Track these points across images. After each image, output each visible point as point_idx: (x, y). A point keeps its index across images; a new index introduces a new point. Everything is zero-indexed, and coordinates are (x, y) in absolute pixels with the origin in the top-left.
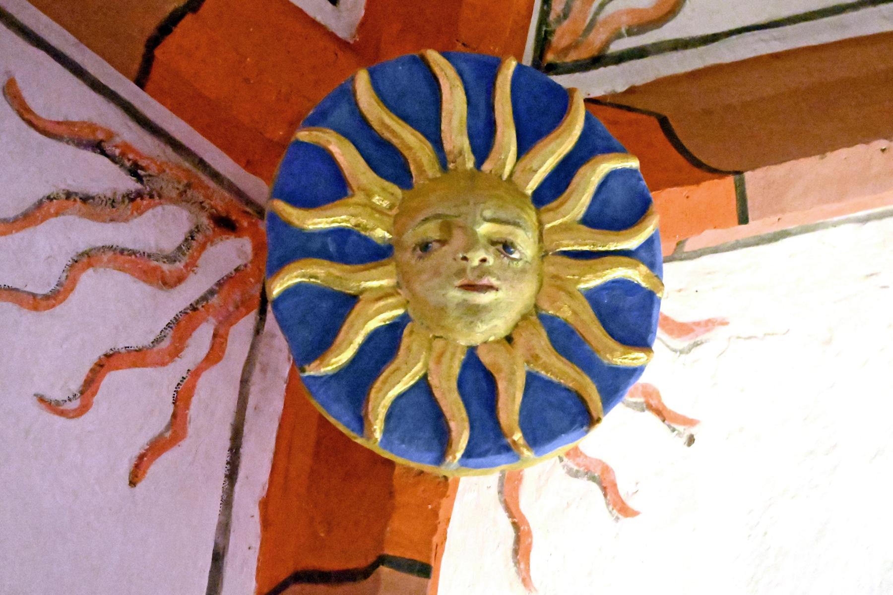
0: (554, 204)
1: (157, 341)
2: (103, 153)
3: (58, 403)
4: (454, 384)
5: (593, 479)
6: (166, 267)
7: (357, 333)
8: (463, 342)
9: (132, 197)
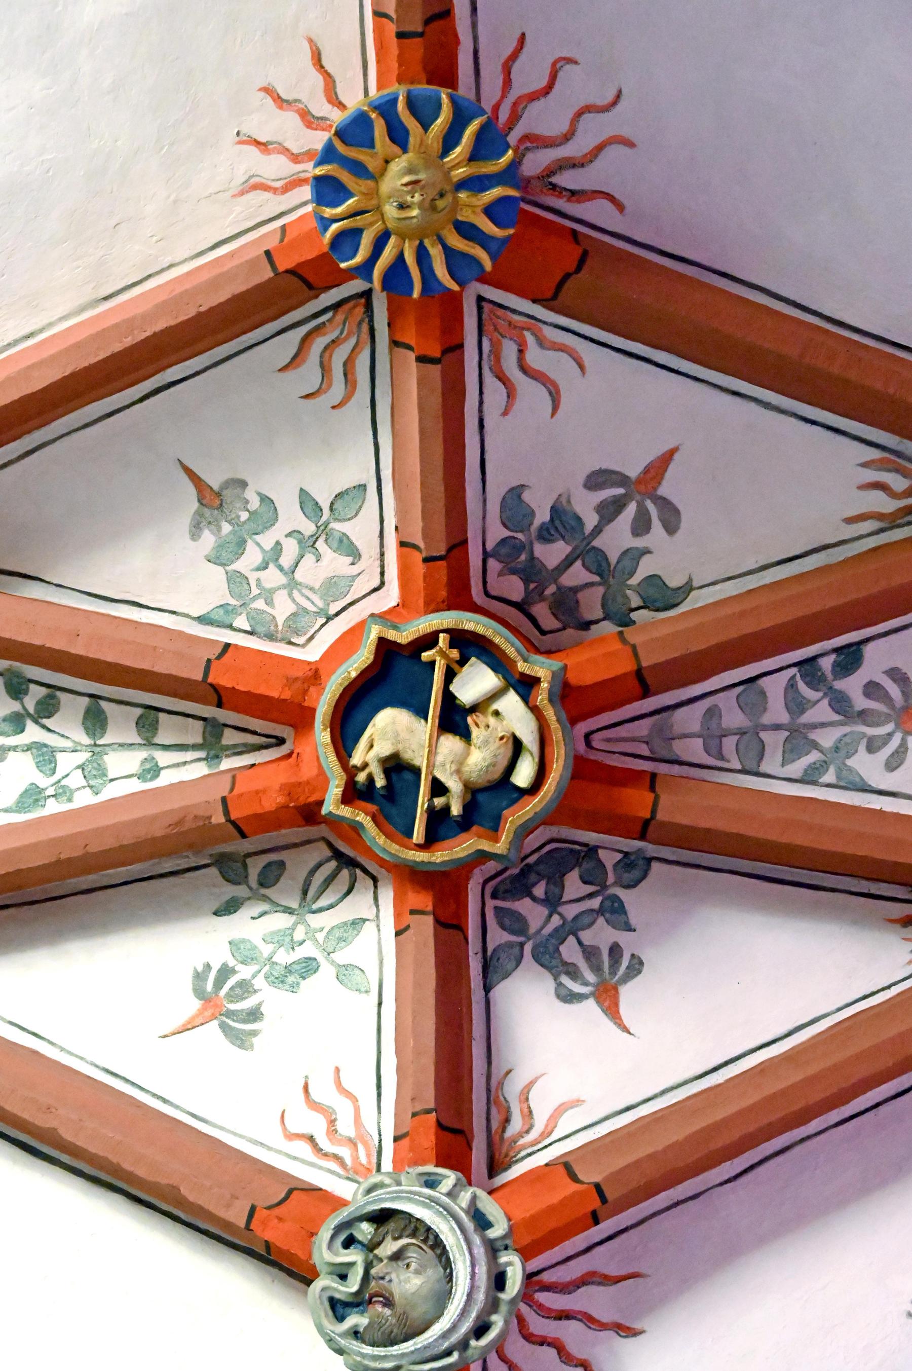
0: (379, 234)
1: (526, 107)
2: (570, 191)
3: (568, 63)
4: (411, 132)
5: (287, 101)
6: (529, 144)
7: (466, 142)
8: (410, 155)
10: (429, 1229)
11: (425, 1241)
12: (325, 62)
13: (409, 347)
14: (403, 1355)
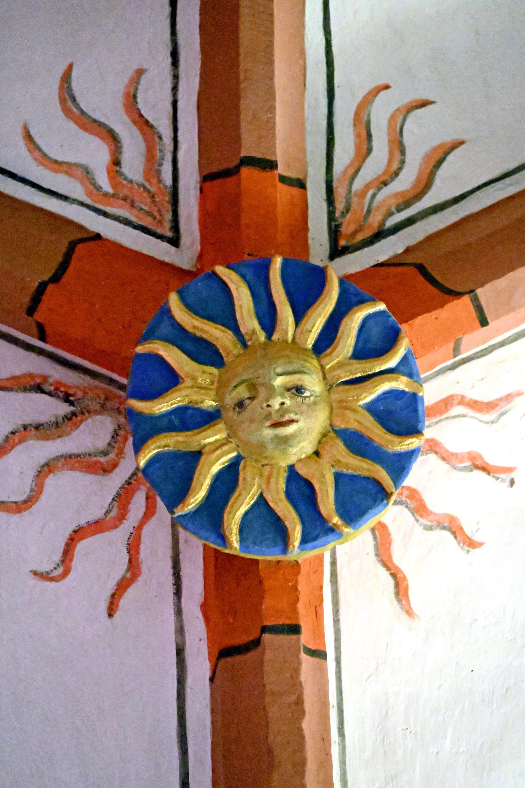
0: (329, 350)
1: (107, 512)
2: (43, 392)
3: (47, 573)
4: (283, 495)
5: (444, 528)
6: (102, 459)
7: (205, 478)
8: (284, 464)
9: (70, 417)
12: (391, 582)
13: (283, 179)
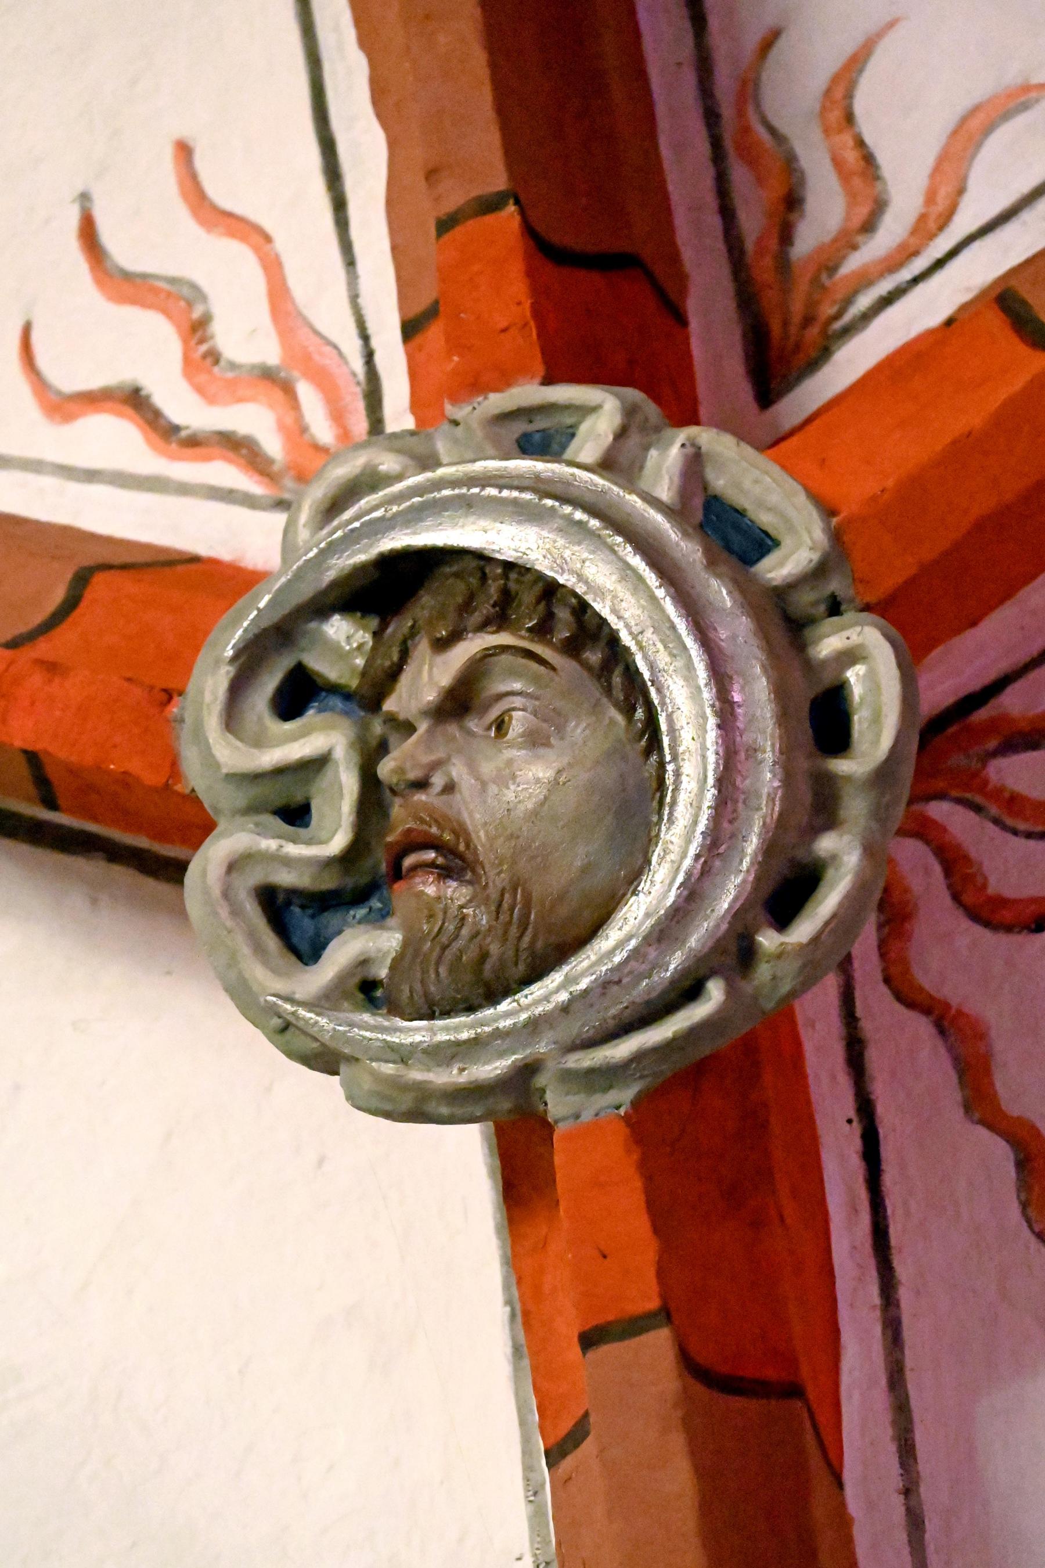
10: (551, 590)
11: (543, 630)
14: (534, 1026)
